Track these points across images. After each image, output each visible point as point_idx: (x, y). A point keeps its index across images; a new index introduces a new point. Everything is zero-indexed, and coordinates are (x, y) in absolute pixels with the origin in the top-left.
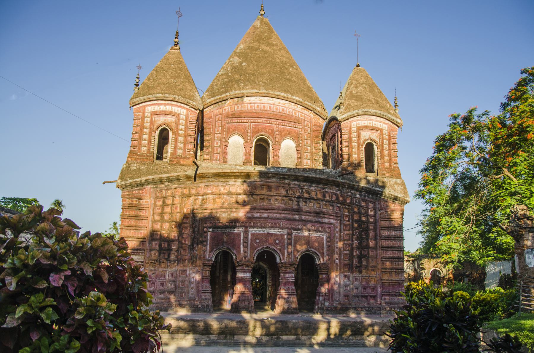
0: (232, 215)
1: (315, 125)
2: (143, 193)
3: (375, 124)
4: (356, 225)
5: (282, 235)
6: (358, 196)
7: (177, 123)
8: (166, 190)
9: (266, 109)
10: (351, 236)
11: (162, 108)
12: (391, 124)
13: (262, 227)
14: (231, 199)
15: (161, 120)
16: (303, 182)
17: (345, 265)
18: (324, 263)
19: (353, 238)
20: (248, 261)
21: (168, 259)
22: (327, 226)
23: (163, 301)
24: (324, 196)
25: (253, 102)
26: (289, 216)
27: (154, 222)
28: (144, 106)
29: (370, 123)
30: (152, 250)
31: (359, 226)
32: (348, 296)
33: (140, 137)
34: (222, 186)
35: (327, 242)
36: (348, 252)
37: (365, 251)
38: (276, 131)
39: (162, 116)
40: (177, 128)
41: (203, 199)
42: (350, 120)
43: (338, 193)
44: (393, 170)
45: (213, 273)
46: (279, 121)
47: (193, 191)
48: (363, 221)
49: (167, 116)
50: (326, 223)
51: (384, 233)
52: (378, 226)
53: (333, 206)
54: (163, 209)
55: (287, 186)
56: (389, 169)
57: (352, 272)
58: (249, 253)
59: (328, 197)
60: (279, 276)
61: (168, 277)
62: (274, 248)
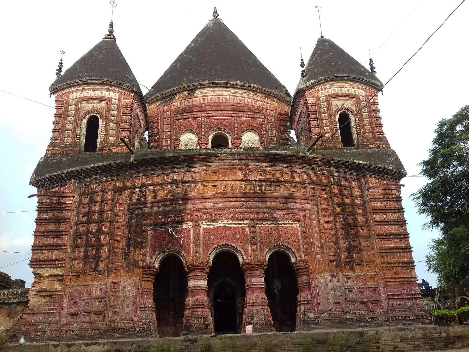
0: (178, 207)
1: (280, 113)
2: (64, 190)
3: (348, 91)
4: (338, 210)
6: (336, 174)
7: (108, 109)
8: (94, 184)
9: (221, 101)
11: (91, 93)
12: (368, 88)
13: (216, 220)
14: (176, 189)
15: (89, 106)
16: (264, 162)
17: (331, 261)
18: (302, 261)
20: (201, 264)
21: (96, 270)
22: (300, 212)
23: (88, 326)
24: (293, 177)
25: (205, 95)
26: (250, 204)
27: (79, 223)
28: (68, 92)
29: (342, 90)
30: (74, 259)
31: (343, 210)
32: (339, 303)
33: (63, 126)
34: (165, 174)
35: (303, 232)
37: (355, 241)
38: (235, 124)
39: (89, 102)
41: (141, 192)
42: (316, 88)
43: (310, 171)
44: (379, 140)
45: (156, 285)
46: (236, 112)
47: (129, 184)
48: (346, 204)
51: (377, 217)
52: (368, 209)
53: (305, 188)
54: (90, 208)
55: (244, 168)
56: (372, 139)
57: (340, 270)
58: (202, 254)
60: (244, 282)
61: (95, 292)
62: (234, 245)
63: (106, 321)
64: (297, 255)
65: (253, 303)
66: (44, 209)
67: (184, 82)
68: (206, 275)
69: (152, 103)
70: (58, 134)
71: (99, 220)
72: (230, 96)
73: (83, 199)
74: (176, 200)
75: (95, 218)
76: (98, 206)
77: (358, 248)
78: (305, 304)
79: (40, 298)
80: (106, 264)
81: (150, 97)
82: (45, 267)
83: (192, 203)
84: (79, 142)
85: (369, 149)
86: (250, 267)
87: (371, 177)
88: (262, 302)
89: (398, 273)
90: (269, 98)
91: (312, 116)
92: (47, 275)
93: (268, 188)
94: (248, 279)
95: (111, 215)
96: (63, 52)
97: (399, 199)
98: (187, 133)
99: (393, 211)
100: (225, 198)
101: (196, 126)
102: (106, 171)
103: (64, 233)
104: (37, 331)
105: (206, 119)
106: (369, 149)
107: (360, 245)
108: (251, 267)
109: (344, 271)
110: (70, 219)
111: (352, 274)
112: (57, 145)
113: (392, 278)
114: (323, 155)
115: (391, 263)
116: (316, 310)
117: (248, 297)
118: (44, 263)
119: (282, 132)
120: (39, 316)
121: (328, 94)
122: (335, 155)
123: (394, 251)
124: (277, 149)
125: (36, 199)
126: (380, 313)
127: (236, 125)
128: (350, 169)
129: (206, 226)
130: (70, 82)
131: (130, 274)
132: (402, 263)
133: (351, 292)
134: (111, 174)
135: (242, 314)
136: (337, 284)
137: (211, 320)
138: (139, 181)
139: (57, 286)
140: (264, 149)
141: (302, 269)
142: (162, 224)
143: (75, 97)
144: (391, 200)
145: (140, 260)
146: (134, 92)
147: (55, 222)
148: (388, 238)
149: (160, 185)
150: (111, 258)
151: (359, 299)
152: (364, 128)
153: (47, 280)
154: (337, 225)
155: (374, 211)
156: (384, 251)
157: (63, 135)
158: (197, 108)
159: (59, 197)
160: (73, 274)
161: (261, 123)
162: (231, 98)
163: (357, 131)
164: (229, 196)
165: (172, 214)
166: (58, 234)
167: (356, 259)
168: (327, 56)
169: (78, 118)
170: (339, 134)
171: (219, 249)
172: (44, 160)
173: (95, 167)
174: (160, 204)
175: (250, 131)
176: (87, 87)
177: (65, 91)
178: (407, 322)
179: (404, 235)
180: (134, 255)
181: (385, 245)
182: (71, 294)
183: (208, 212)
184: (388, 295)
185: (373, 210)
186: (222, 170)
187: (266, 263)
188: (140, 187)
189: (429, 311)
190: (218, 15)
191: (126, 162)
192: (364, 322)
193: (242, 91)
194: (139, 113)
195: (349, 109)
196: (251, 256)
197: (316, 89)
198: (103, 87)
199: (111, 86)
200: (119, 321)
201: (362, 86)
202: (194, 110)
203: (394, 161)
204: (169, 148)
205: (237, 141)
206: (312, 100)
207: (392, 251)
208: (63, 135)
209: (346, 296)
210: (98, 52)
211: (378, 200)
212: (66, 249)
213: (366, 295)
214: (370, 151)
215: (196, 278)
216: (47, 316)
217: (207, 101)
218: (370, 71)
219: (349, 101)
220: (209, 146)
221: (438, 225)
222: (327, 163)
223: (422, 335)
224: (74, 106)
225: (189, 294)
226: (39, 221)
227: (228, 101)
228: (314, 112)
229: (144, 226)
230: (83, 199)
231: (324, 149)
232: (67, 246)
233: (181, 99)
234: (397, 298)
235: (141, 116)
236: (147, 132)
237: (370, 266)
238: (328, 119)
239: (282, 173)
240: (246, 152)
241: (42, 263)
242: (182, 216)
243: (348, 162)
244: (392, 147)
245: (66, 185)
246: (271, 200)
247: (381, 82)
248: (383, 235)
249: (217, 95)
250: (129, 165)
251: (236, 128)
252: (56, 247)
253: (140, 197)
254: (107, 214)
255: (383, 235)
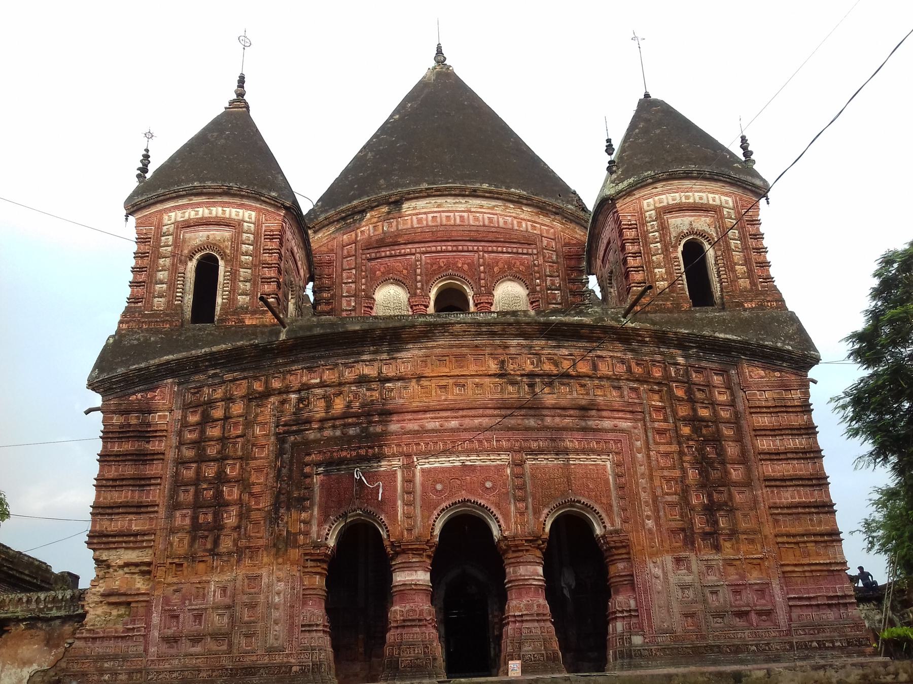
0: (371, 429)
1: (566, 244)
2: (153, 398)
3: (701, 198)
4: (686, 430)
5: (499, 469)
6: (681, 360)
7: (237, 242)
8: (209, 386)
9: (452, 222)
10: (676, 456)
11: (203, 212)
12: (739, 192)
13: (446, 452)
14: (368, 393)
15: (200, 236)
16: (538, 338)
17: (673, 532)
18: (617, 532)
19: (682, 462)
22: (610, 436)
23: (199, 662)
24: (595, 367)
25: (422, 212)
26: (512, 422)
27: (181, 462)
28: (161, 212)
29: (687, 198)
30: (173, 531)
31: (696, 430)
32: (692, 615)
33: (151, 276)
34: (346, 365)
35: (618, 476)
36: (675, 498)
37: (721, 492)
39: (201, 228)
40: (236, 250)
41: (300, 400)
43: (629, 356)
44: (762, 293)
46: (483, 244)
47: (276, 384)
48: (702, 420)
49: (211, 227)
50: (606, 431)
51: (764, 444)
52: (746, 428)
53: (619, 388)
54: (203, 432)
55: (500, 351)
56: (751, 290)
57: (693, 549)
58: (419, 519)
59: (604, 369)
60: (503, 574)
61: (214, 595)
62: (483, 502)
63: (235, 652)
64: (606, 520)
65: (522, 616)
66: (114, 436)
67: (380, 188)
68: (429, 561)
69: (320, 229)
70: (140, 291)
71: (219, 456)
72: (471, 212)
73: (189, 414)
74: (369, 414)
75: (212, 451)
76: (218, 428)
77: (727, 506)
78: (623, 617)
79: (106, 608)
80: (234, 540)
81: (316, 217)
82: (116, 548)
83: (398, 421)
84: (181, 306)
85: (745, 310)
86: (515, 546)
87: (749, 366)
88: (538, 615)
89: (809, 555)
90: (546, 215)
91: (629, 247)
92: (121, 563)
93: (547, 390)
94: (511, 569)
95: (243, 446)
96: (149, 135)
97: (806, 408)
98: (387, 284)
99: (795, 432)
100: (463, 409)
101: (405, 272)
102: (233, 360)
103: (153, 481)
104: (102, 672)
105: (423, 257)
106: (745, 310)
107: (731, 501)
108: (516, 546)
109: (700, 551)
110: (164, 454)
111: (716, 557)
112: (140, 313)
113: (796, 565)
114: (653, 323)
115: (794, 536)
116: (646, 629)
117: (511, 605)
118: (114, 540)
119: (573, 281)
120: (106, 643)
121: (661, 205)
122: (678, 323)
123: (800, 510)
124: (563, 313)
125: (99, 415)
126: (774, 634)
127: (482, 268)
128: (709, 349)
129: (427, 466)
130: (163, 191)
131: (280, 560)
132: (815, 535)
133: (716, 593)
134: (243, 366)
135: (500, 637)
136: (686, 578)
137: (438, 650)
138: (296, 379)
139: (140, 584)
140: (538, 313)
141: (617, 548)
142: (342, 461)
143: (173, 221)
144: (791, 410)
145: (300, 532)
146: (286, 208)
147: (135, 460)
148: (786, 486)
149: (336, 386)
150: (243, 530)
151: (731, 606)
152: (733, 270)
153: (121, 572)
154: (684, 462)
155: (758, 433)
156: (779, 511)
157: (150, 293)
158: (406, 237)
159: (142, 412)
160: (170, 561)
161: (531, 263)
162: (471, 217)
163: (719, 276)
164: (470, 406)
165: (360, 442)
166: (141, 482)
167: (723, 529)
168: (658, 131)
169: (179, 259)
170: (685, 282)
171: (452, 510)
172: (115, 341)
173: (212, 354)
174: (338, 423)
175: (510, 280)
176: (196, 200)
177: (153, 209)
178: (829, 653)
179: (818, 479)
180: (287, 523)
181: (780, 498)
182: (167, 601)
183: (430, 437)
184: (790, 599)
185: (755, 430)
186: (456, 356)
187: (546, 536)
188: (299, 391)
189: (873, 629)
190: (445, 59)
191: (271, 343)
192: (742, 652)
193: (493, 203)
194: (295, 249)
195: (702, 234)
196: (516, 523)
197: (637, 196)
198: (226, 199)
199: (242, 197)
200: (259, 652)
201: (728, 189)
202: (401, 240)
203: (796, 334)
204: (353, 314)
205: (484, 299)
206: (629, 218)
207: (794, 511)
208: (150, 293)
209: (705, 601)
210: (215, 134)
211: (765, 410)
212: (157, 512)
213: (744, 598)
214: (746, 314)
215: (408, 567)
216: (120, 644)
217: (425, 222)
218: (743, 159)
219: (703, 219)
220: (431, 309)
221: (886, 460)
222: (661, 339)
223: (858, 677)
224: (170, 238)
225: (395, 598)
226: (104, 458)
227: (467, 223)
228: (634, 241)
229: (307, 465)
230: (189, 414)
231: (656, 312)
232: (158, 505)
233: (375, 220)
234: (807, 605)
235: (299, 254)
236: (311, 284)
237: (752, 541)
238: (662, 253)
239: (574, 360)
240: (502, 319)
241: (110, 539)
242: (380, 446)
243: (703, 337)
244: (791, 306)
245: (157, 388)
246: (552, 412)
247: (764, 181)
248: (776, 480)
249: (444, 212)
250: (278, 347)
251: (482, 275)
252: (138, 508)
253: (299, 409)
254: (235, 444)
255: (776, 480)
